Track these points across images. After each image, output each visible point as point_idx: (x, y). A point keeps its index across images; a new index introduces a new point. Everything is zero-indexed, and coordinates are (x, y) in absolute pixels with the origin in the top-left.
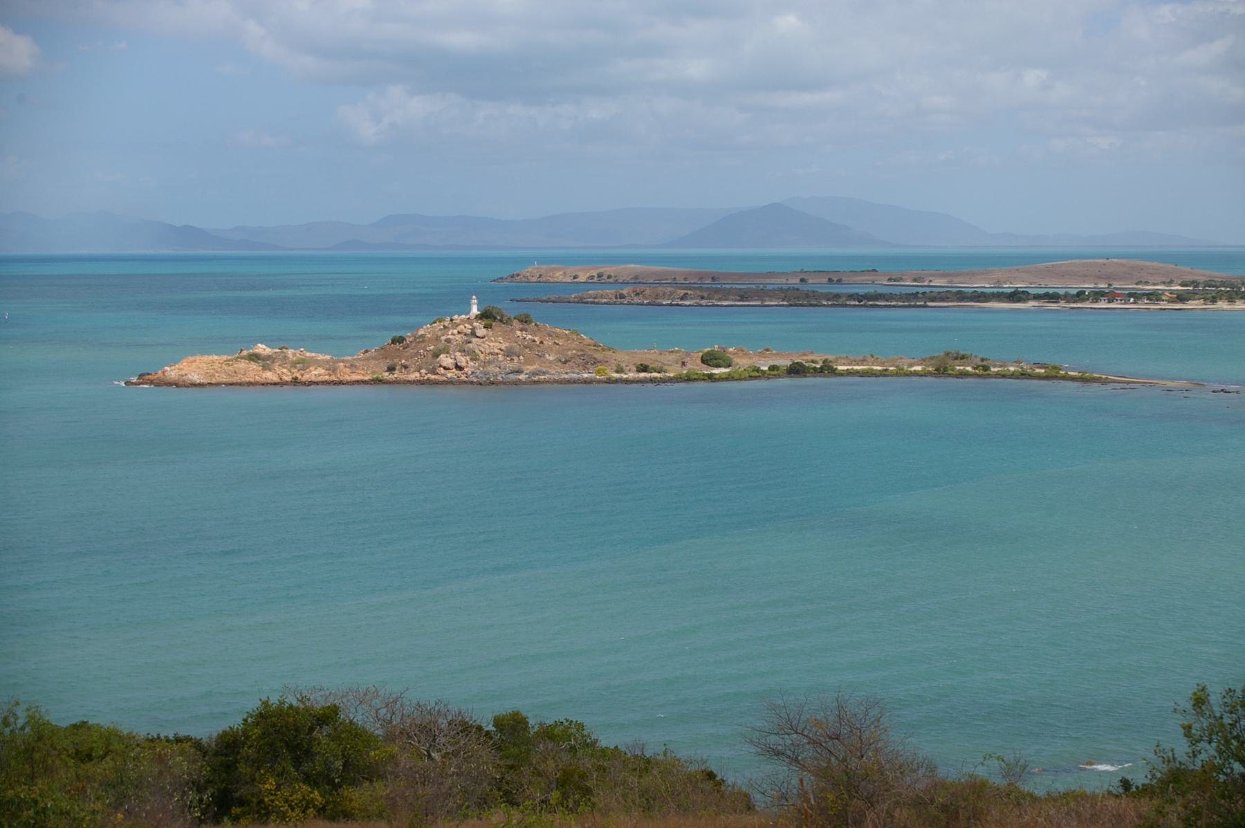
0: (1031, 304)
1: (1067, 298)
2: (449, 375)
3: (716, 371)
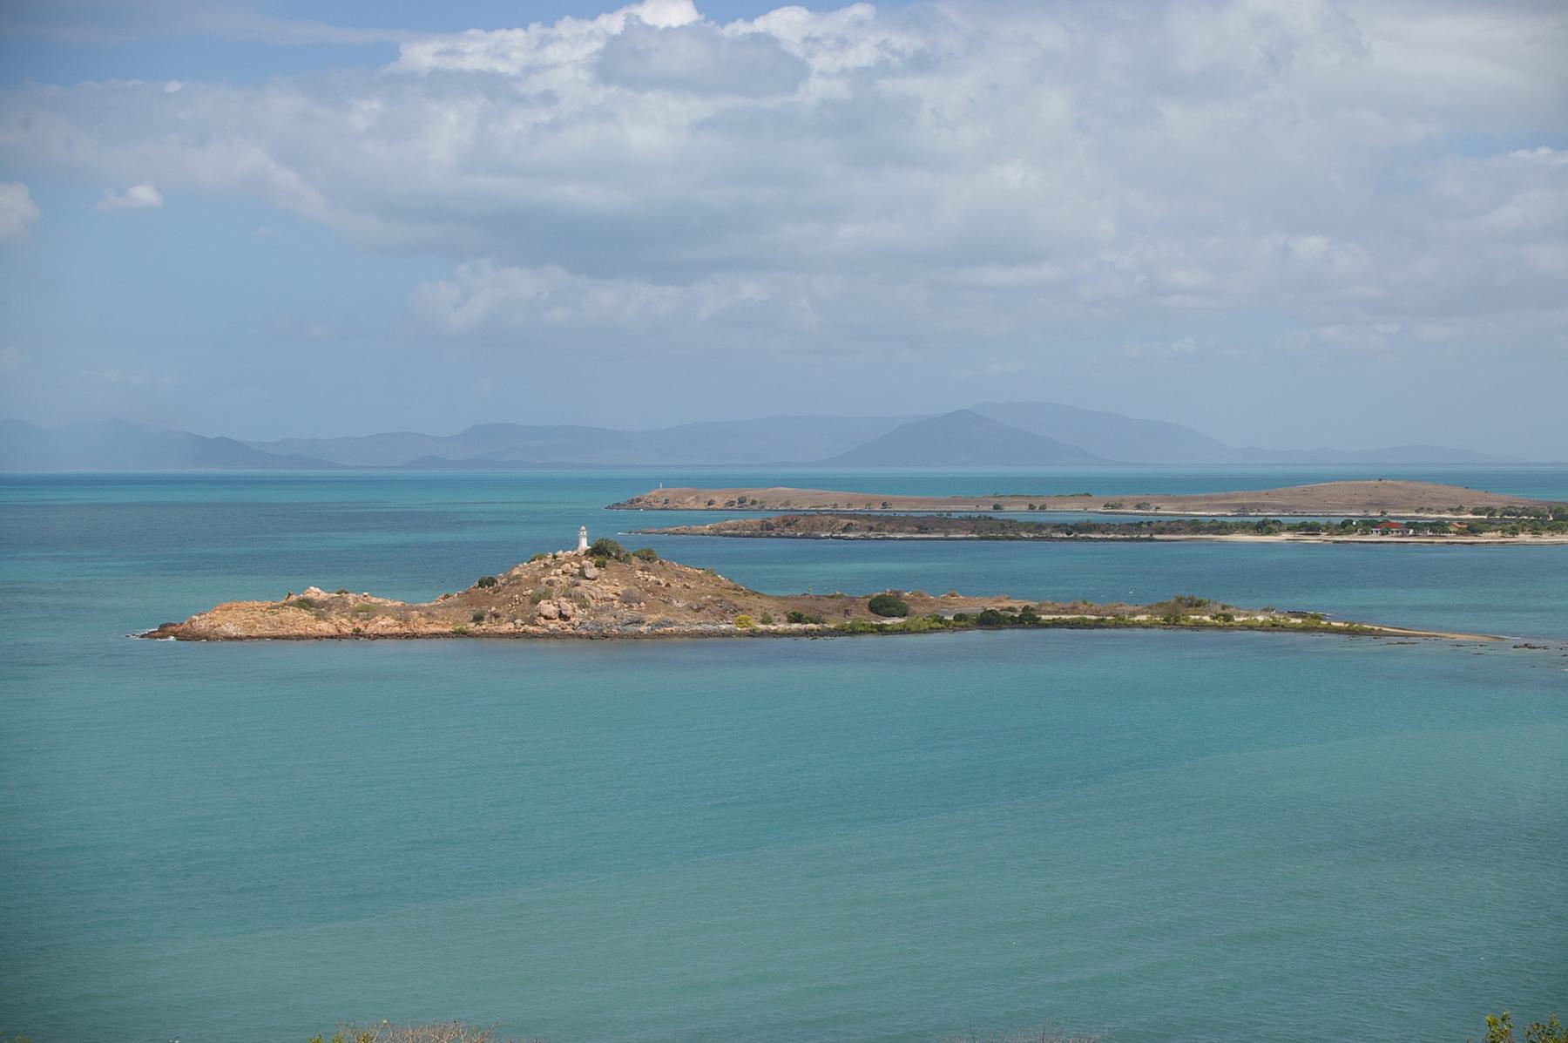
0: (1285, 536)
1: (1328, 528)
2: (552, 626)
3: (888, 621)
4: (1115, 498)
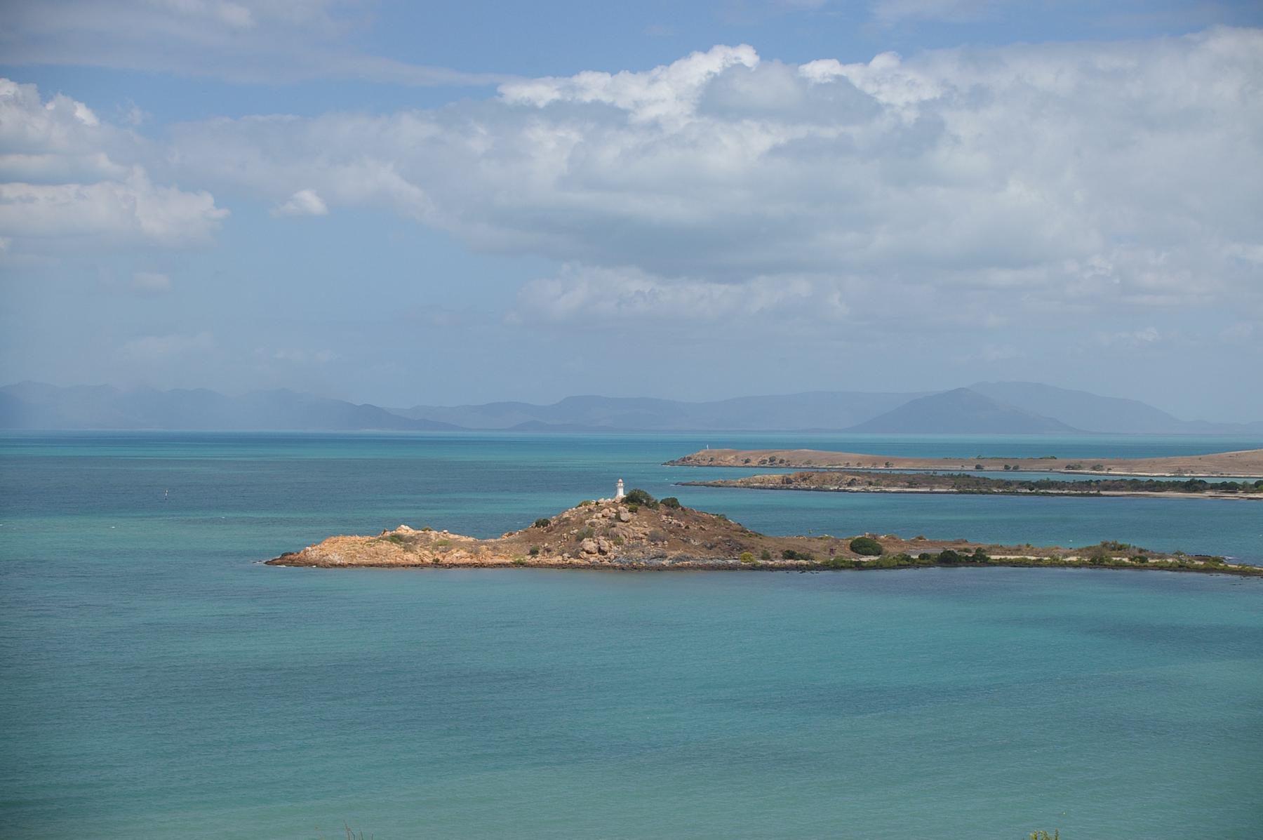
0: (1209, 493)
2: (592, 559)
3: (865, 559)
4: (1073, 460)
